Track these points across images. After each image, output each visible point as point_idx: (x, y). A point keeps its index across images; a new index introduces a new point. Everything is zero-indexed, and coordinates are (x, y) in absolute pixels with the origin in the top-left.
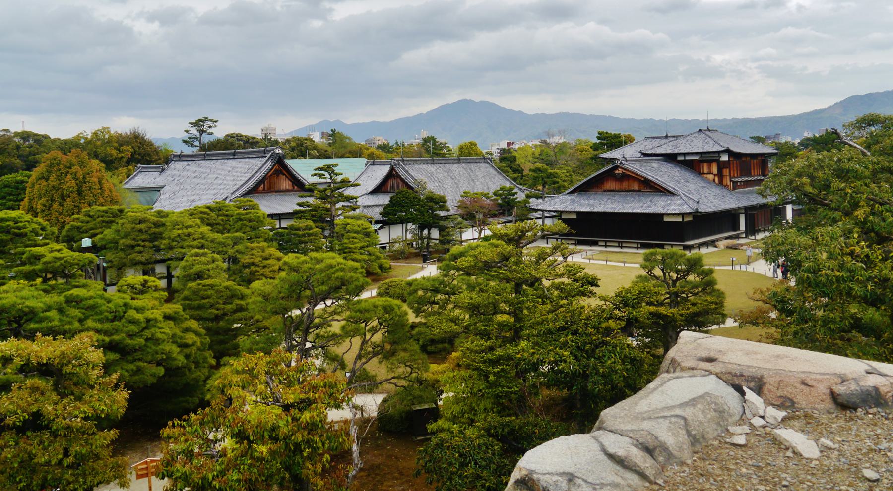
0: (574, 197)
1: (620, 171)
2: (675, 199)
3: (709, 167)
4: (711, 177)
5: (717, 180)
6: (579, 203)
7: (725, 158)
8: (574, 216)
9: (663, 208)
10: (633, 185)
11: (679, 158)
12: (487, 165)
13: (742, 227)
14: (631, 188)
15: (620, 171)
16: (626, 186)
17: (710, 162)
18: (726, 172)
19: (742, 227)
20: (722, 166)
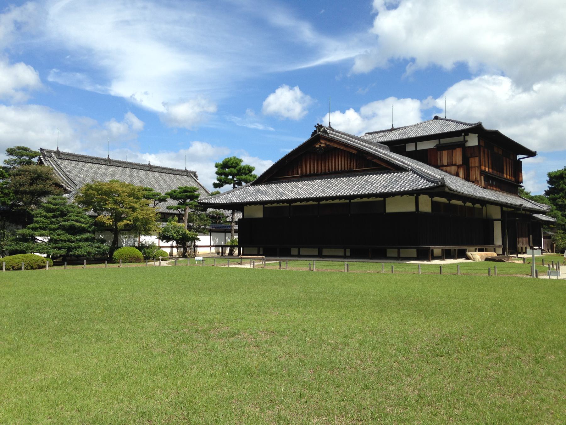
0: (260, 187)
1: (323, 144)
2: (404, 174)
3: (451, 157)
4: (454, 169)
5: (461, 172)
6: (266, 193)
7: (473, 141)
8: (260, 215)
9: (385, 187)
10: (341, 163)
11: (410, 148)
12: (189, 179)
13: (498, 241)
14: (339, 168)
15: (323, 144)
16: (331, 165)
17: (451, 147)
18: (474, 162)
19: (498, 241)
20: (468, 153)
